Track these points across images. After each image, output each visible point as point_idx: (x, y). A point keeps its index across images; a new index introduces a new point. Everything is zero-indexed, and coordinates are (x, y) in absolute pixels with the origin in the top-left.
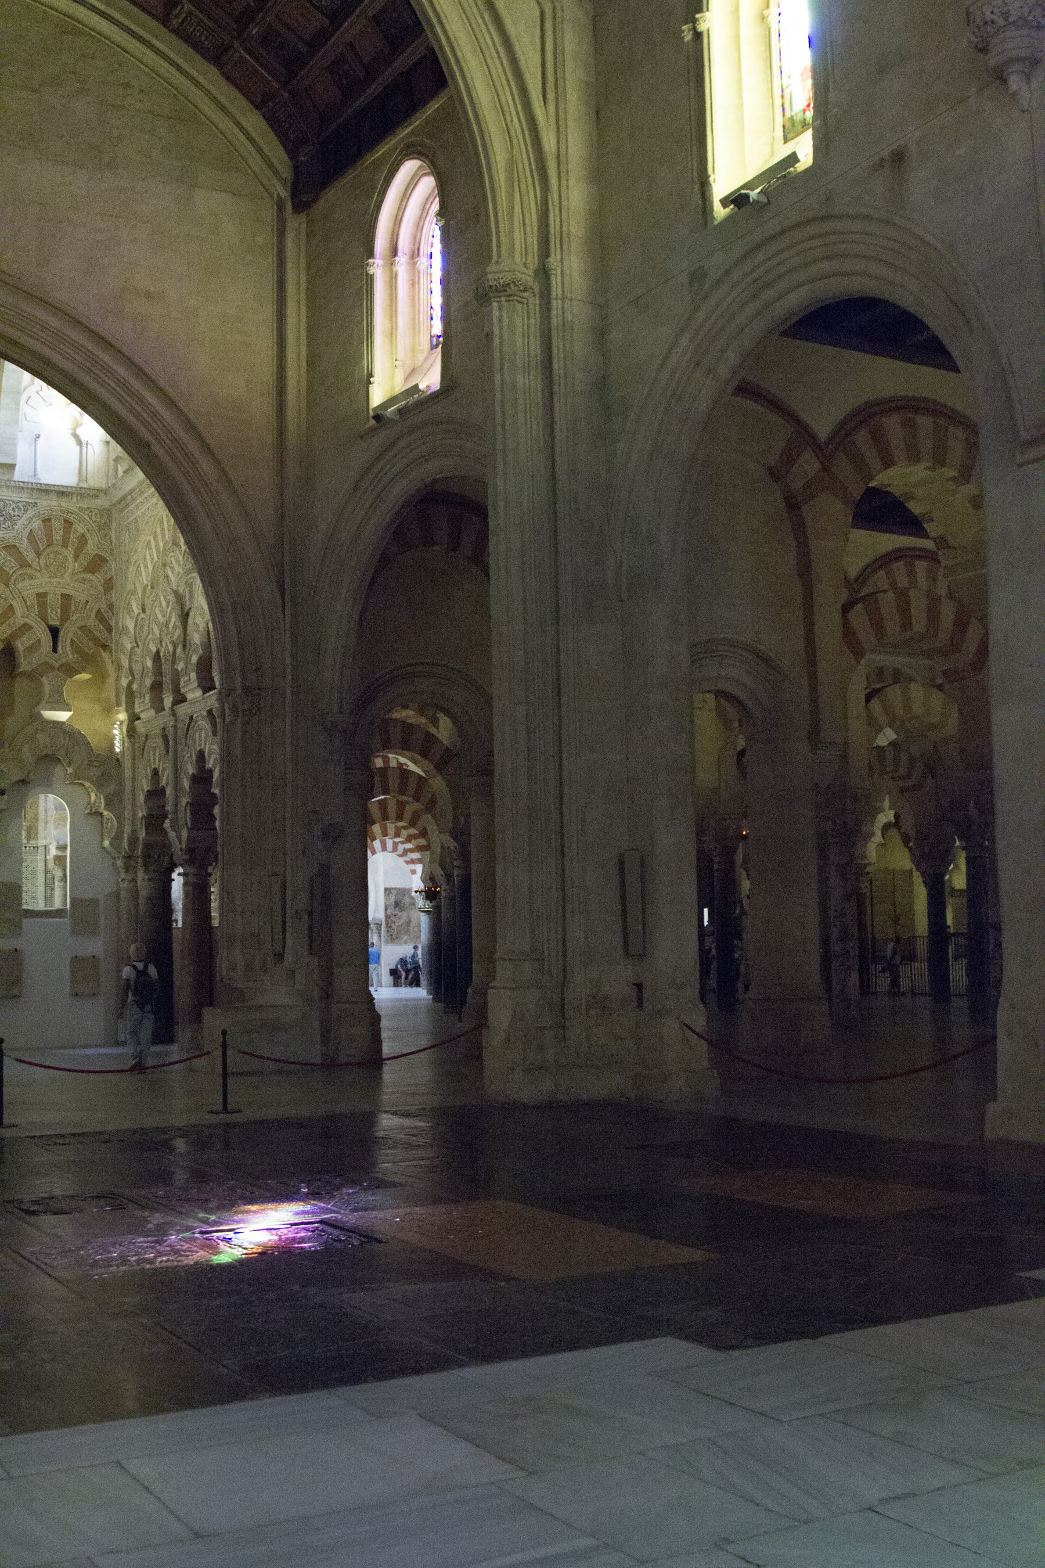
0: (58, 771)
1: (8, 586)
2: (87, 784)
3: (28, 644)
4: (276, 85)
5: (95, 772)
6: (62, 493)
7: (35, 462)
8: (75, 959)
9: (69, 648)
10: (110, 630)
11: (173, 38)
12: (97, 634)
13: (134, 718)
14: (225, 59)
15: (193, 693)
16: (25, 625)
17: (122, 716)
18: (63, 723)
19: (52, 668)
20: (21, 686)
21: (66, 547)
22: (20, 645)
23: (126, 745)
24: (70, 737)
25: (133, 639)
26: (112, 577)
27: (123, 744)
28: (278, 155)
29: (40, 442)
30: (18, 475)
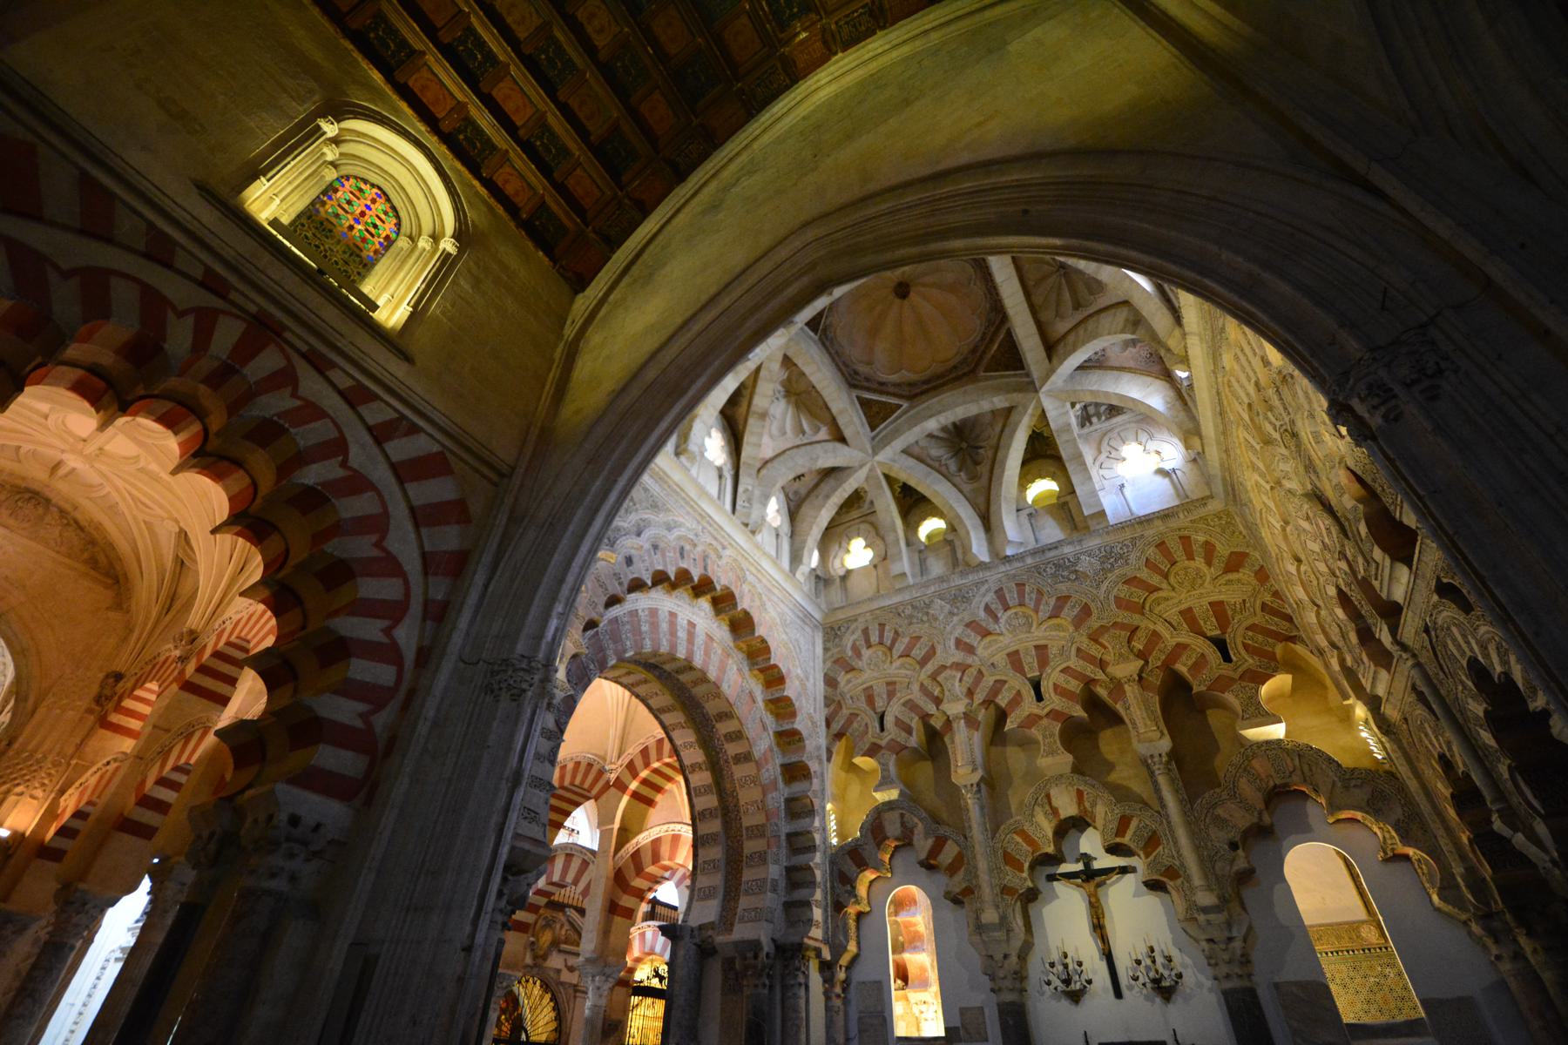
0: (1311, 808)
1: (1143, 614)
2: (1359, 815)
3: (1190, 663)
5: (1361, 795)
6: (1165, 515)
7: (1128, 505)
9: (1243, 652)
10: (1289, 619)
12: (1274, 628)
13: (1374, 704)
15: (1399, 584)
16: (1178, 645)
17: (1361, 711)
18: (1280, 741)
19: (1232, 680)
20: (1215, 718)
21: (1194, 559)
22: (1182, 668)
23: (1387, 745)
24: (1299, 755)
25: (1311, 605)
26: (1262, 566)
27: (1385, 748)
29: (1125, 490)
30: (1112, 519)
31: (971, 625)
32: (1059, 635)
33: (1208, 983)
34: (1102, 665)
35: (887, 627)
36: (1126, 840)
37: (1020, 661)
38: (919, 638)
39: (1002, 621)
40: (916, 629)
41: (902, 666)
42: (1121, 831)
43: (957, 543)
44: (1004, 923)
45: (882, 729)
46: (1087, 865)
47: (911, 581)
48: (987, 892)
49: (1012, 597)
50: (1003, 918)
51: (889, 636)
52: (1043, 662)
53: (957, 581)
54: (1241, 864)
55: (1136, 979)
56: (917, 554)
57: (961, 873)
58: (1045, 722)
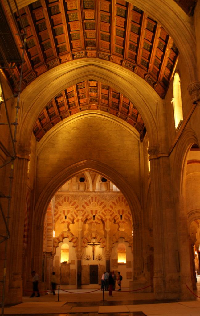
4: (135, 122)
8: (127, 272)
11: (120, 119)
14: (127, 120)
28: (137, 133)
31: (86, 203)
32: (99, 208)
33: (104, 258)
34: (105, 216)
35: (69, 199)
36: (100, 241)
37: (92, 212)
38: (75, 203)
39: (91, 204)
40: (76, 201)
41: (72, 207)
42: (100, 240)
43: (87, 185)
44: (81, 251)
45: (66, 219)
46: (94, 244)
47: (76, 191)
48: (80, 246)
49: (94, 199)
50: (81, 250)
51: (70, 201)
52: (96, 213)
53: (85, 193)
54: (113, 246)
55: (97, 258)
56: (78, 185)
57: (76, 244)
58: (94, 223)
